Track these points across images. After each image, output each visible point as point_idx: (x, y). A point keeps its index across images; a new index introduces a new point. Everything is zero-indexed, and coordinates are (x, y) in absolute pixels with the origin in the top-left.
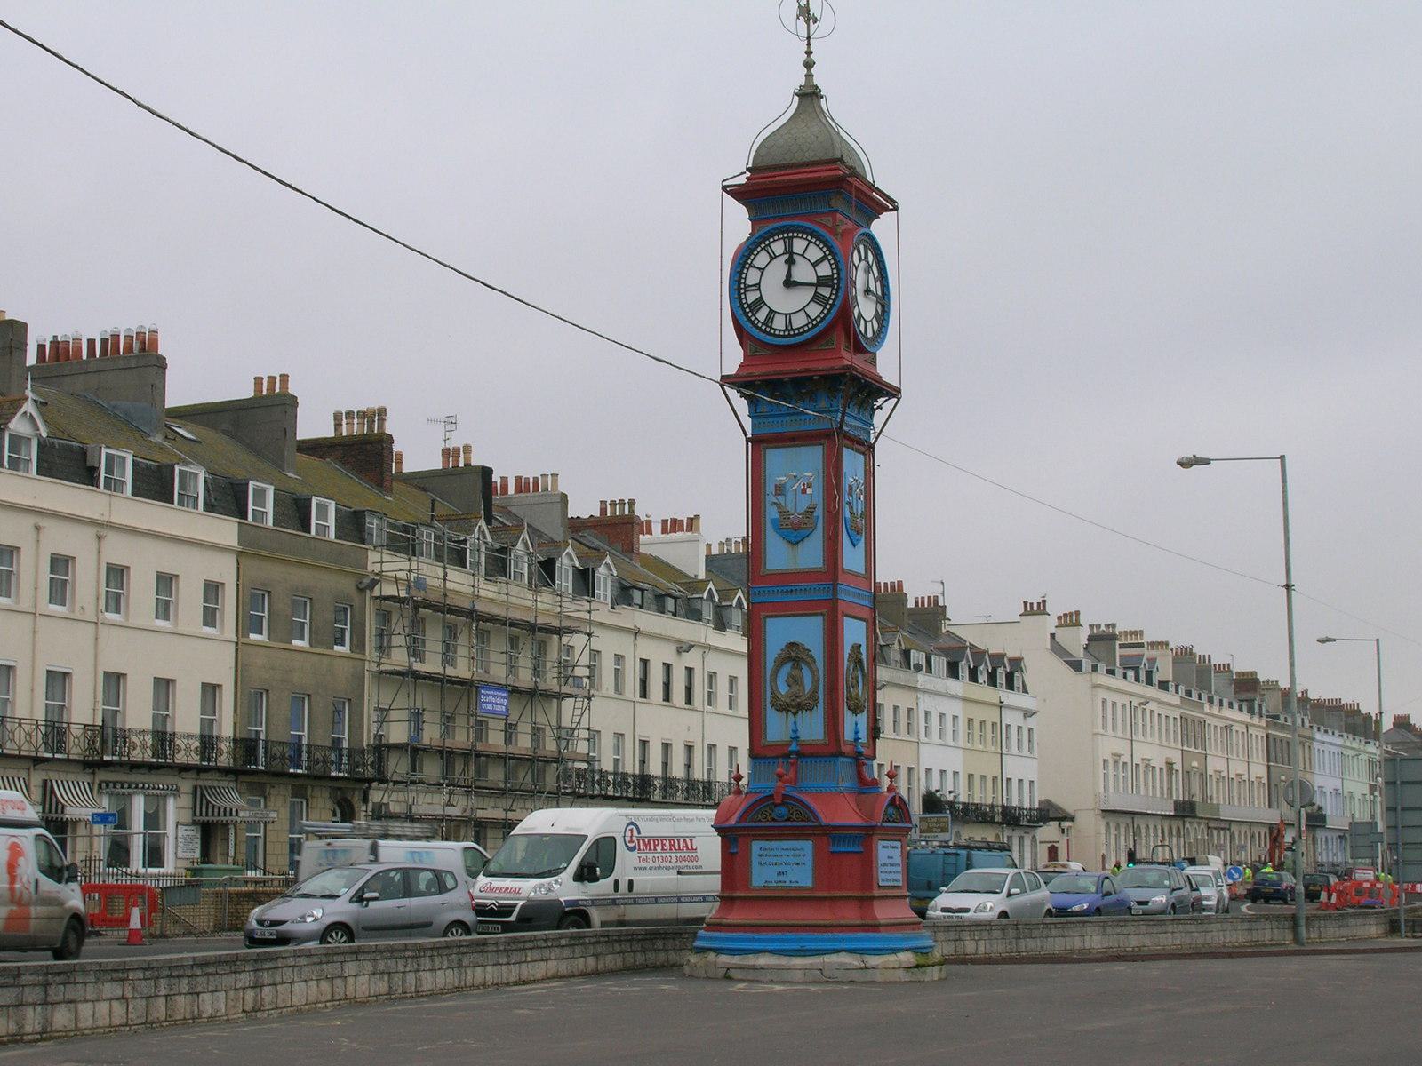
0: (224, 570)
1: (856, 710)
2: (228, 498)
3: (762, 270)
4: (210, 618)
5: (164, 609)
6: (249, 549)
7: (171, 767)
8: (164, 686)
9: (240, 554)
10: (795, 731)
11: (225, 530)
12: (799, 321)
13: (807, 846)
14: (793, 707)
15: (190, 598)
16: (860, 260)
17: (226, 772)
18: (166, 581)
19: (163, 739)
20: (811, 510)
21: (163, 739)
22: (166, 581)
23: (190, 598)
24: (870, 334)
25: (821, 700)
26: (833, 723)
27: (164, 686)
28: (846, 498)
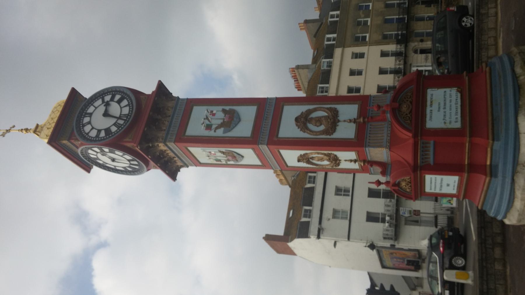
0: (349, 51)
1: (333, 120)
2: (329, 53)
3: (115, 166)
4: (361, 56)
5: (360, 73)
6: (343, 44)
7: (405, 52)
8: (382, 72)
9: (344, 47)
10: (351, 161)
11: (338, 52)
12: (129, 157)
13: (430, 92)
14: (336, 160)
15: (358, 64)
16: (89, 123)
17: (406, 47)
18: (353, 73)
19: (395, 72)
20: (220, 152)
21: (395, 72)
22: (353, 73)
23: (358, 64)
24: (126, 111)
25: (330, 152)
26: (344, 144)
27: (382, 72)
28: (211, 133)
